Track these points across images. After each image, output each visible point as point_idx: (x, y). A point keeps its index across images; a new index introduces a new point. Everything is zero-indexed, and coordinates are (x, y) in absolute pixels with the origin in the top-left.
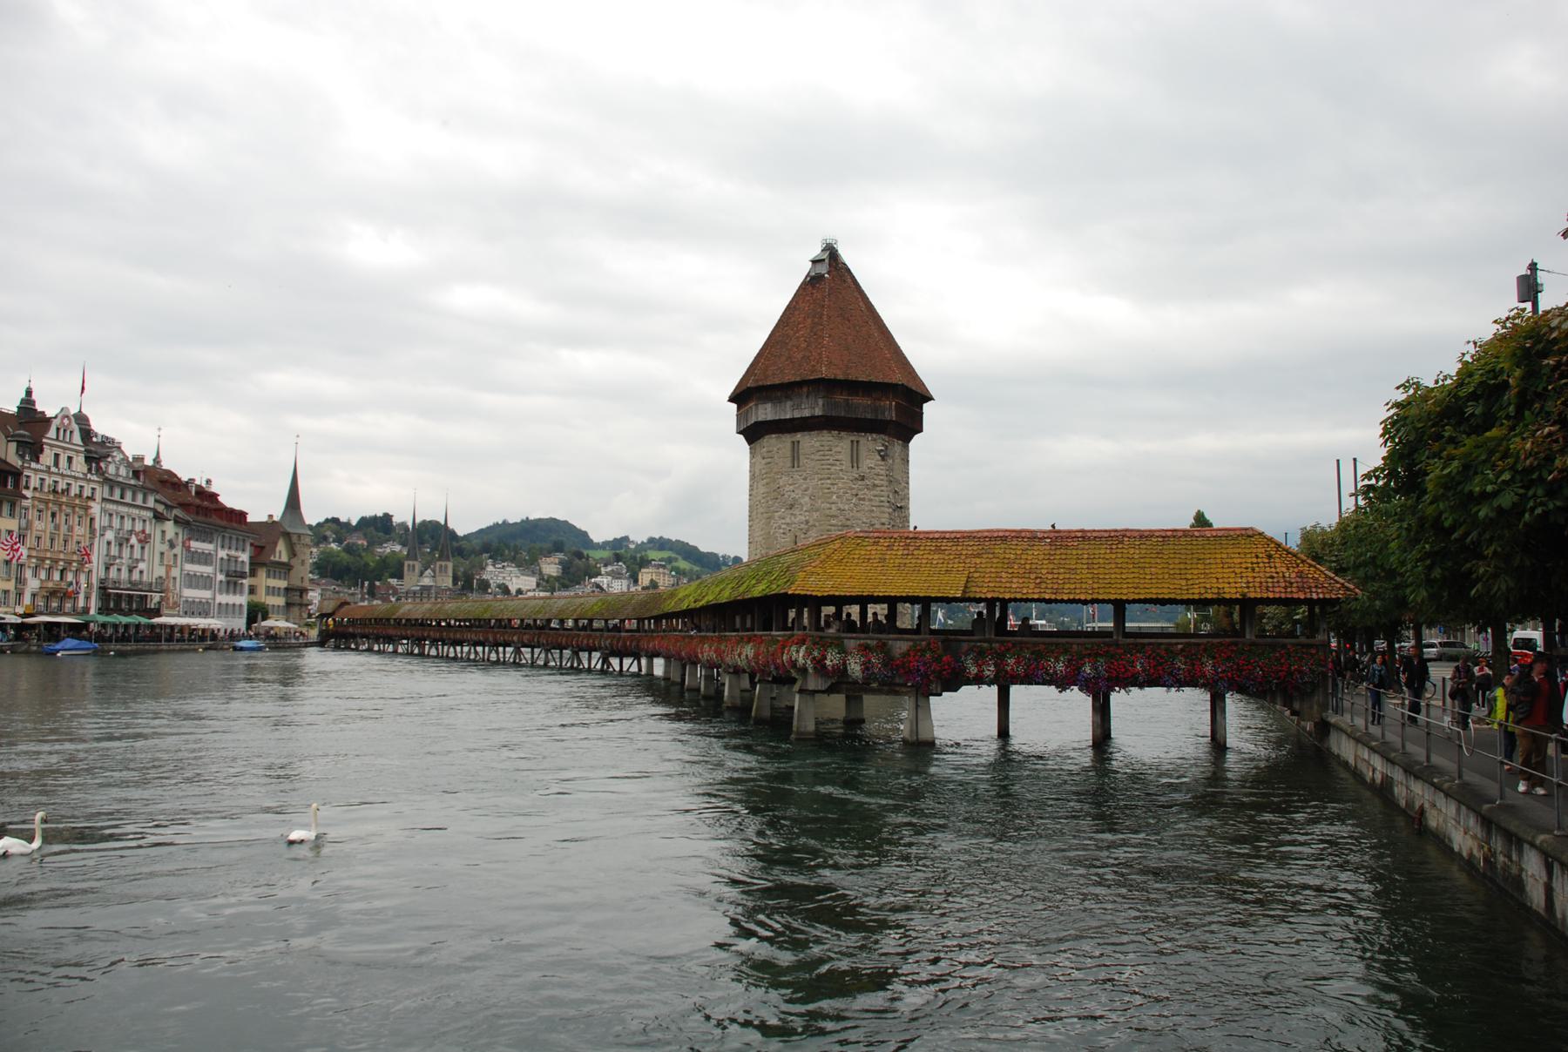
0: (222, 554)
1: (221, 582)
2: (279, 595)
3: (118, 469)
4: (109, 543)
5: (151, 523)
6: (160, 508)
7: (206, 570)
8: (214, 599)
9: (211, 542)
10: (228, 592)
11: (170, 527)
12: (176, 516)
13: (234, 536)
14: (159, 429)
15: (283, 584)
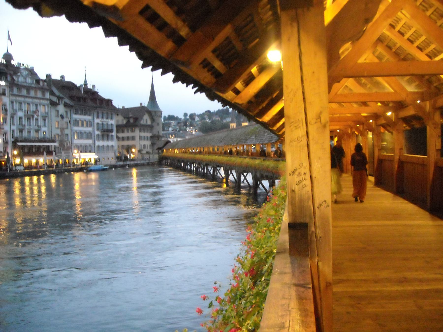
0: (97, 121)
1: (98, 135)
2: (147, 140)
3: (25, 79)
4: (20, 118)
5: (48, 107)
6: (55, 99)
7: (90, 129)
8: (94, 144)
9: (89, 115)
10: (103, 140)
11: (61, 109)
12: (64, 101)
13: (109, 112)
14: (85, 67)
15: (149, 135)
